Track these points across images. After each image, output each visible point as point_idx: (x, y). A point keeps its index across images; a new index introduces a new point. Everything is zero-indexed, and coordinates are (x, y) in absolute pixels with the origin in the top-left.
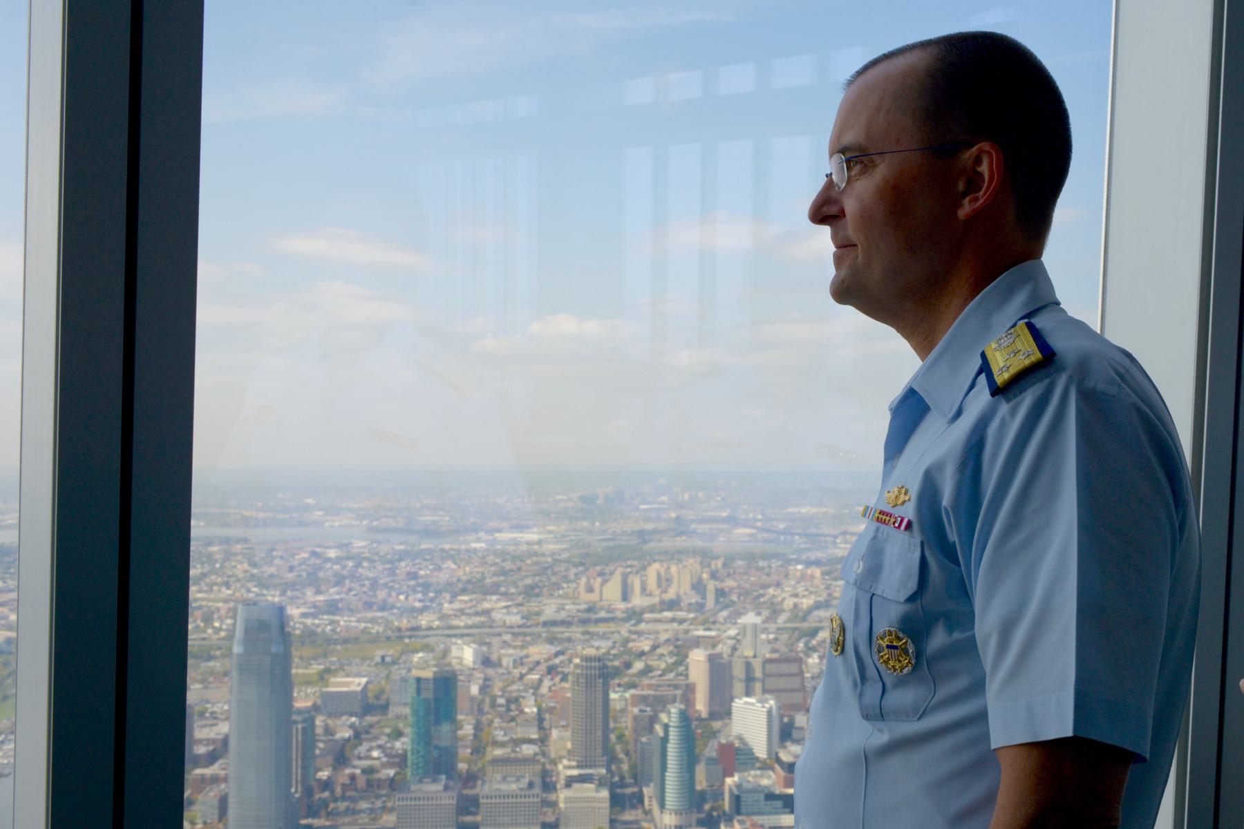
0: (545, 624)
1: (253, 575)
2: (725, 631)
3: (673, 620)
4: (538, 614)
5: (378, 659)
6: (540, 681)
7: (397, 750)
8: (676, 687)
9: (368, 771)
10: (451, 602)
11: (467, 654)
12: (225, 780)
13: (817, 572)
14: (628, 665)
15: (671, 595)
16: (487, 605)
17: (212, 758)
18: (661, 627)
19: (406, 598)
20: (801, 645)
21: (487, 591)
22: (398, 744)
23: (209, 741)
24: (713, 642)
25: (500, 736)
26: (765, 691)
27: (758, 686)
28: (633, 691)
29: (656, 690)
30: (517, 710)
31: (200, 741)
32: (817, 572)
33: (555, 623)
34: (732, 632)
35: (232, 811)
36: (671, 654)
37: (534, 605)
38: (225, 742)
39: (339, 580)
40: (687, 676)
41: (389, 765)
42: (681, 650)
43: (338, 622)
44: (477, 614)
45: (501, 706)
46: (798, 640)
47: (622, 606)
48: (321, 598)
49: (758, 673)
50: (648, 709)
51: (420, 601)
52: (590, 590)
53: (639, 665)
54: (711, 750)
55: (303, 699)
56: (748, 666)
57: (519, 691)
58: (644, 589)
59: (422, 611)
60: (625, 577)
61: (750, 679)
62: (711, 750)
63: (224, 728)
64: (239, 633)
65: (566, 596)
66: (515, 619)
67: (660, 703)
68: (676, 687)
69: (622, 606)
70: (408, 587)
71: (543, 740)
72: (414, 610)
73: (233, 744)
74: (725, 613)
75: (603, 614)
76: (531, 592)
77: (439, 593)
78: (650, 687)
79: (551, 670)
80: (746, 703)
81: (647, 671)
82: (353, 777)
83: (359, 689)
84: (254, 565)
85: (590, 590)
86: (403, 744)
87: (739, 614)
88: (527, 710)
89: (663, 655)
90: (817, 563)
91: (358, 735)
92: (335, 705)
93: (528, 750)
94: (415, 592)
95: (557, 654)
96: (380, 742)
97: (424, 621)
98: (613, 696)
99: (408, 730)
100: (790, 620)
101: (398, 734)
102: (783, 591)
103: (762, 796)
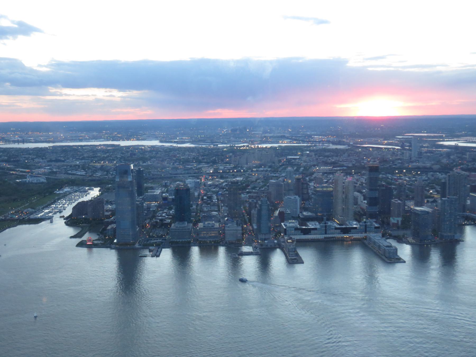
1: (122, 157)
2: (281, 174)
5: (164, 184)
7: (171, 214)
9: (161, 220)
10: (188, 165)
11: (190, 182)
12: (115, 223)
13: (313, 154)
19: (173, 164)
21: (199, 162)
22: (171, 212)
23: (110, 210)
24: (277, 178)
28: (250, 194)
29: (257, 194)
30: (210, 201)
31: (107, 211)
32: (313, 154)
34: (284, 175)
40: (268, 189)
43: (150, 172)
45: (205, 199)
46: (307, 177)
47: (246, 166)
48: (145, 164)
50: (255, 200)
51: (177, 165)
53: (252, 186)
57: (211, 194)
70: (174, 160)
71: (219, 211)
78: (255, 193)
80: (288, 198)
81: (254, 188)
82: (157, 222)
83: (158, 193)
84: (123, 154)
86: (173, 212)
88: (214, 201)
89: (259, 182)
90: (313, 151)
94: (176, 162)
95: (224, 182)
96: (165, 211)
99: (174, 208)
101: (170, 209)
102: (302, 161)
103: (294, 229)
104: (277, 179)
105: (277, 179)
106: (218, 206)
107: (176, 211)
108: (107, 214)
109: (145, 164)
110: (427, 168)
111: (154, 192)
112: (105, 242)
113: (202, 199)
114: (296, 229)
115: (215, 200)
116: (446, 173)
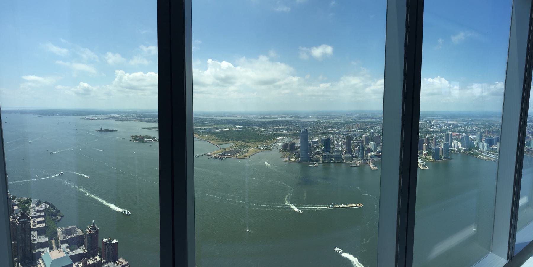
0: (342, 132)
3: (359, 131)
4: (341, 131)
6: (341, 140)
8: (361, 141)
9: (318, 152)
14: (354, 138)
15: (359, 128)
16: (334, 129)
17: (297, 149)
18: (358, 132)
20: (379, 135)
21: (334, 128)
23: (297, 147)
25: (336, 147)
26: (374, 141)
27: (373, 140)
33: (343, 132)
35: (301, 156)
36: (360, 136)
37: (340, 130)
38: (300, 146)
39: (313, 126)
41: (321, 151)
42: (361, 135)
44: (332, 131)
47: (352, 129)
48: (311, 128)
49: (373, 139)
52: (348, 127)
53: (355, 138)
54: (366, 149)
55: (310, 141)
56: (371, 138)
58: (355, 127)
59: (325, 130)
60: (353, 125)
61: (372, 140)
62: (366, 149)
63: (299, 145)
64: (301, 133)
65: (344, 128)
66: (338, 131)
67: (358, 143)
68: (361, 141)
69: (352, 129)
71: (342, 148)
72: (324, 130)
73: (300, 147)
74: (368, 131)
75: (350, 131)
76: (340, 128)
77: (327, 128)
79: (343, 138)
85: (348, 127)
87: (370, 131)
91: (317, 147)
92: (314, 142)
93: (340, 149)
97: (325, 131)
98: (352, 142)
100: (378, 131)
101: (322, 147)
104: (366, 135)
105: (366, 135)
106: (342, 146)
107: (324, 147)
108: (296, 148)
109: (311, 128)
110: (437, 131)
111: (315, 140)
112: (295, 160)
113: (335, 143)
114: (375, 156)
115: (340, 144)
116: (444, 133)
